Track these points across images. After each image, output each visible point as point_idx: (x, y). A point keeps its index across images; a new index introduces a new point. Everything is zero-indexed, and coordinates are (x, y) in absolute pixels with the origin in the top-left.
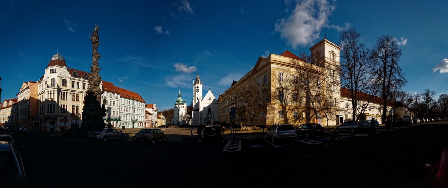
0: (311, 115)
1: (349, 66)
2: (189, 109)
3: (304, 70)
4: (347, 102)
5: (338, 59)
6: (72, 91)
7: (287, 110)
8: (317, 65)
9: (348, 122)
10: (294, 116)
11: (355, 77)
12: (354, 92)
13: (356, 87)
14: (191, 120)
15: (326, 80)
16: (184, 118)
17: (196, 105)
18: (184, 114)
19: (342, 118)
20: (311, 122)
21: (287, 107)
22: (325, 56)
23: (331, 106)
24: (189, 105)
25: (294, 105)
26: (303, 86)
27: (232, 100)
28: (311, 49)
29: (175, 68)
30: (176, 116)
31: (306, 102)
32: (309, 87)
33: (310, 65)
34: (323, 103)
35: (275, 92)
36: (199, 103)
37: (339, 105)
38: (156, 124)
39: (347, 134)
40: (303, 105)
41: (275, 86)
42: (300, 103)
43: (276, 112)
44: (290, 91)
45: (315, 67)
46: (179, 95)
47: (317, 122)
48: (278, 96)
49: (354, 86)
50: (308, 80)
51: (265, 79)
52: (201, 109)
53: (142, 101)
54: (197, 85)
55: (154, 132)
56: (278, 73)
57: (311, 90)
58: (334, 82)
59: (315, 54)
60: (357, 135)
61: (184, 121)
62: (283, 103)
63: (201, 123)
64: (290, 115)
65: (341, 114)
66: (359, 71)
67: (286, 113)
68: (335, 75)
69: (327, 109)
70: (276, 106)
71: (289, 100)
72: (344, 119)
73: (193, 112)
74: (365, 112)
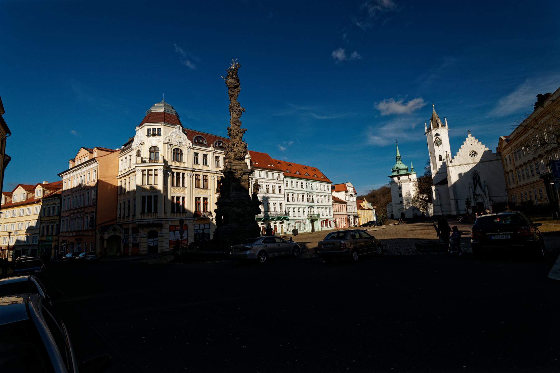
2: (424, 184)
6: (194, 170)
14: (431, 206)
16: (413, 202)
17: (438, 173)
18: (413, 195)
24: (422, 174)
27: (544, 143)
29: (379, 112)
36: (444, 167)
38: (357, 220)
46: (397, 159)
52: (454, 178)
53: (325, 180)
55: (353, 237)
73: (433, 188)
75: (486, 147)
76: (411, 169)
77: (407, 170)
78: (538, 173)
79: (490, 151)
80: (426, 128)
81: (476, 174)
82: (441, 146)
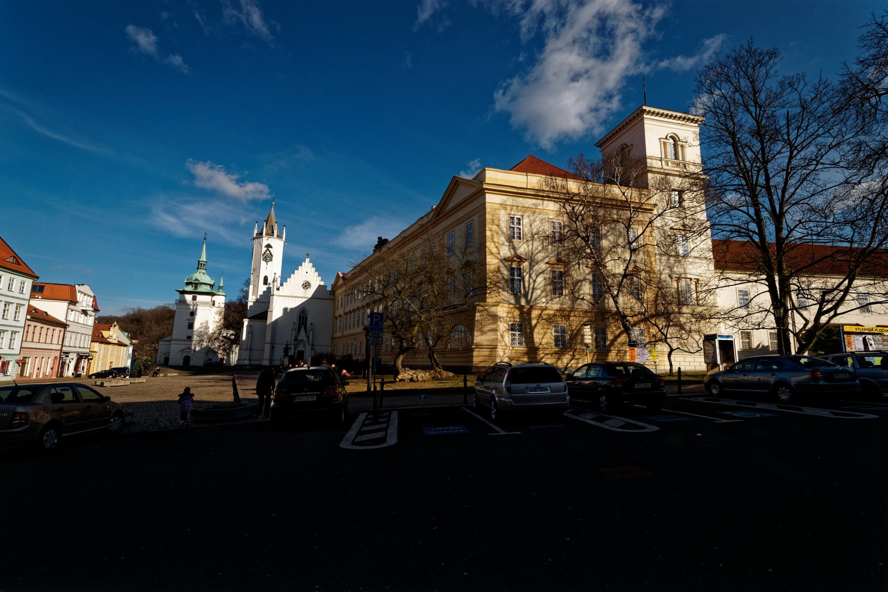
0: (610, 337)
1: (741, 165)
2: (234, 313)
3: (581, 202)
4: (742, 287)
5: (693, 154)
7: (534, 322)
8: (625, 183)
9: (756, 359)
10: (557, 339)
11: (770, 195)
12: (773, 250)
13: (779, 230)
14: (236, 349)
15: (658, 223)
16: (210, 339)
17: (257, 301)
18: (212, 328)
19: (727, 346)
20: (612, 357)
21: (535, 313)
22: (649, 153)
23: (680, 304)
24: (234, 299)
25: (557, 307)
26: (582, 249)
27: (373, 292)
28: (601, 144)
30: (178, 331)
31: (594, 296)
32: (599, 249)
33: (601, 188)
34: (649, 295)
35: (498, 270)
36: (268, 294)
37: (710, 299)
39: (759, 406)
40: (585, 306)
41: (496, 252)
42: (575, 299)
43: (502, 326)
44: (543, 266)
45: (616, 191)
47: (632, 357)
48: (506, 281)
49: (770, 229)
50: (597, 231)
51: (468, 236)
52: (276, 313)
56: (507, 217)
57: (609, 258)
58: (684, 225)
59: (616, 155)
60: (808, 411)
61: (209, 351)
62: (523, 302)
63: (271, 360)
64: (544, 337)
65: (723, 330)
66: (788, 172)
67: (532, 329)
68: (686, 204)
69: (667, 315)
70: (502, 311)
71: (538, 292)
72: (738, 347)
73: (246, 322)
74: (835, 321)
76: (220, 287)
77: (212, 286)
78: (363, 324)
81: (303, 312)
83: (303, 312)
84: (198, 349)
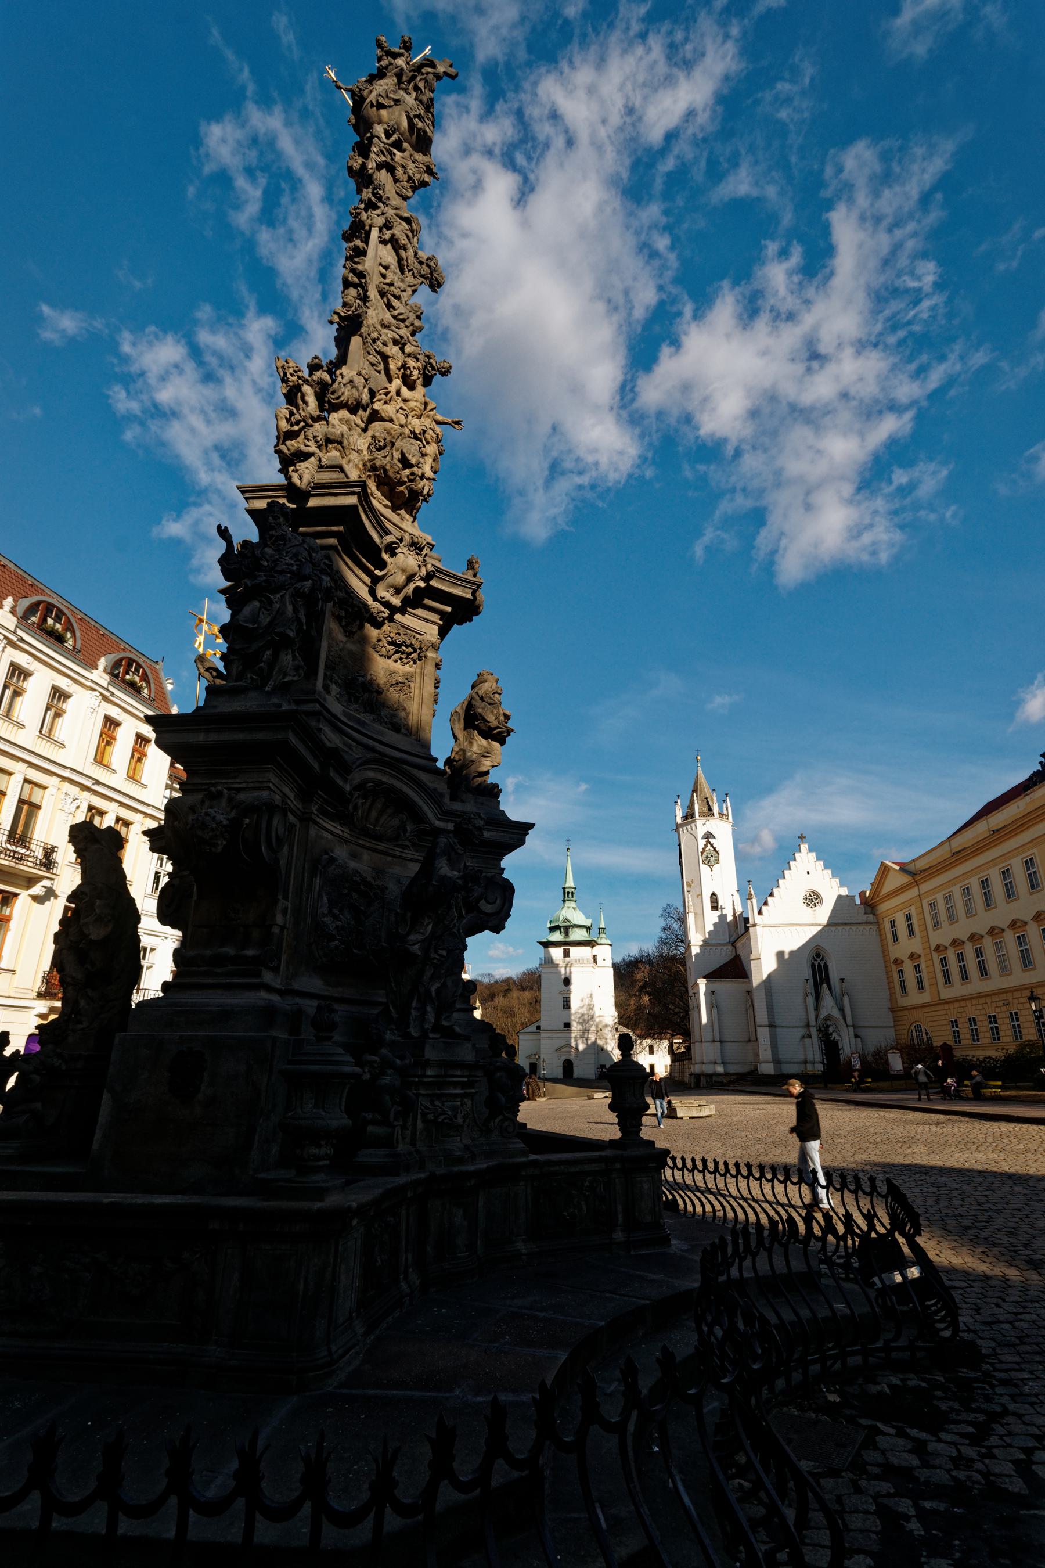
17: (706, 944)
24: (645, 943)
30: (549, 1017)
46: (567, 895)
54: (702, 826)
75: (842, 885)
76: (600, 930)
77: (588, 929)
79: (850, 898)
80: (679, 814)
81: (818, 955)
82: (716, 867)
83: (818, 955)
84: (581, 1047)
